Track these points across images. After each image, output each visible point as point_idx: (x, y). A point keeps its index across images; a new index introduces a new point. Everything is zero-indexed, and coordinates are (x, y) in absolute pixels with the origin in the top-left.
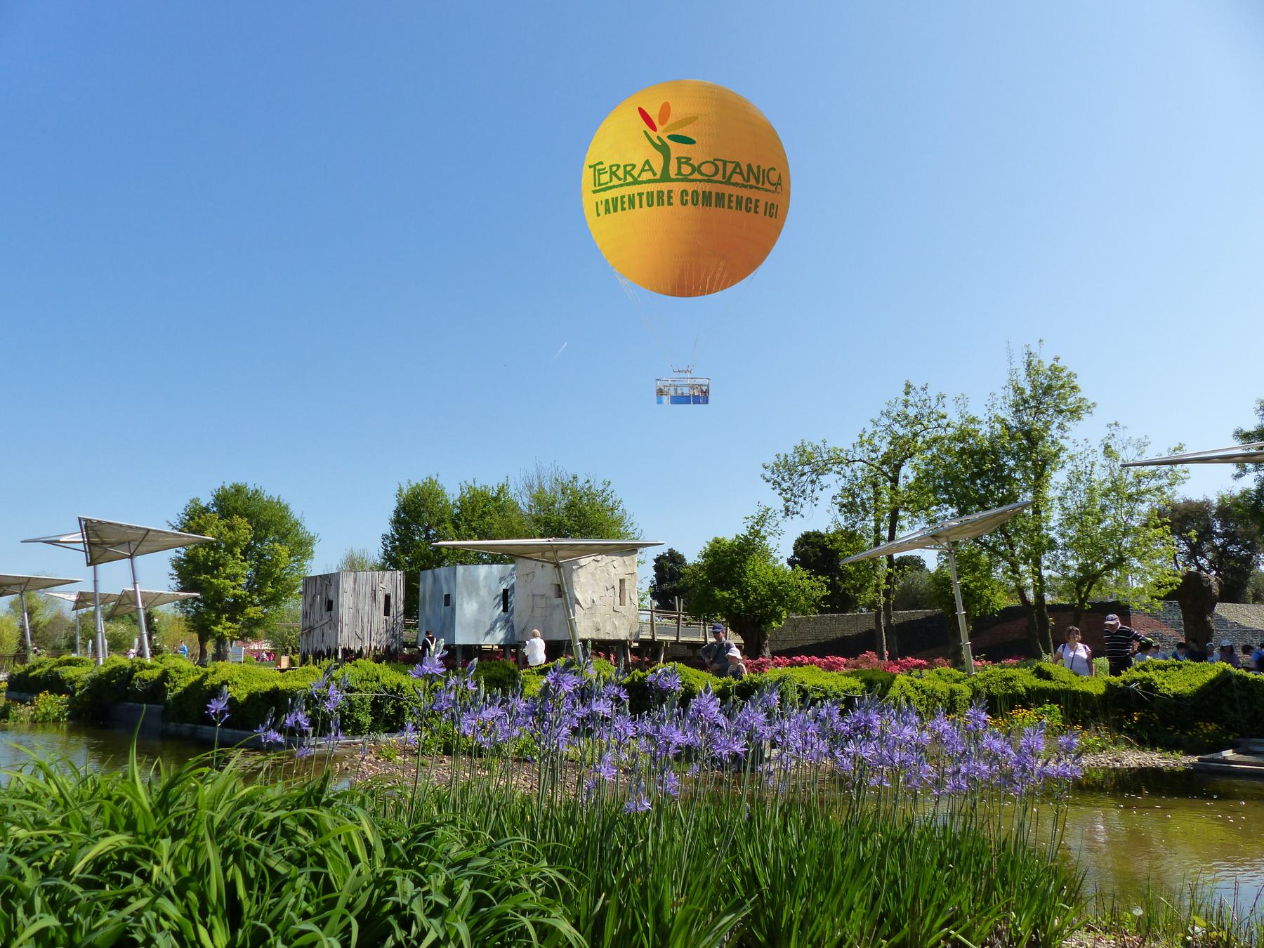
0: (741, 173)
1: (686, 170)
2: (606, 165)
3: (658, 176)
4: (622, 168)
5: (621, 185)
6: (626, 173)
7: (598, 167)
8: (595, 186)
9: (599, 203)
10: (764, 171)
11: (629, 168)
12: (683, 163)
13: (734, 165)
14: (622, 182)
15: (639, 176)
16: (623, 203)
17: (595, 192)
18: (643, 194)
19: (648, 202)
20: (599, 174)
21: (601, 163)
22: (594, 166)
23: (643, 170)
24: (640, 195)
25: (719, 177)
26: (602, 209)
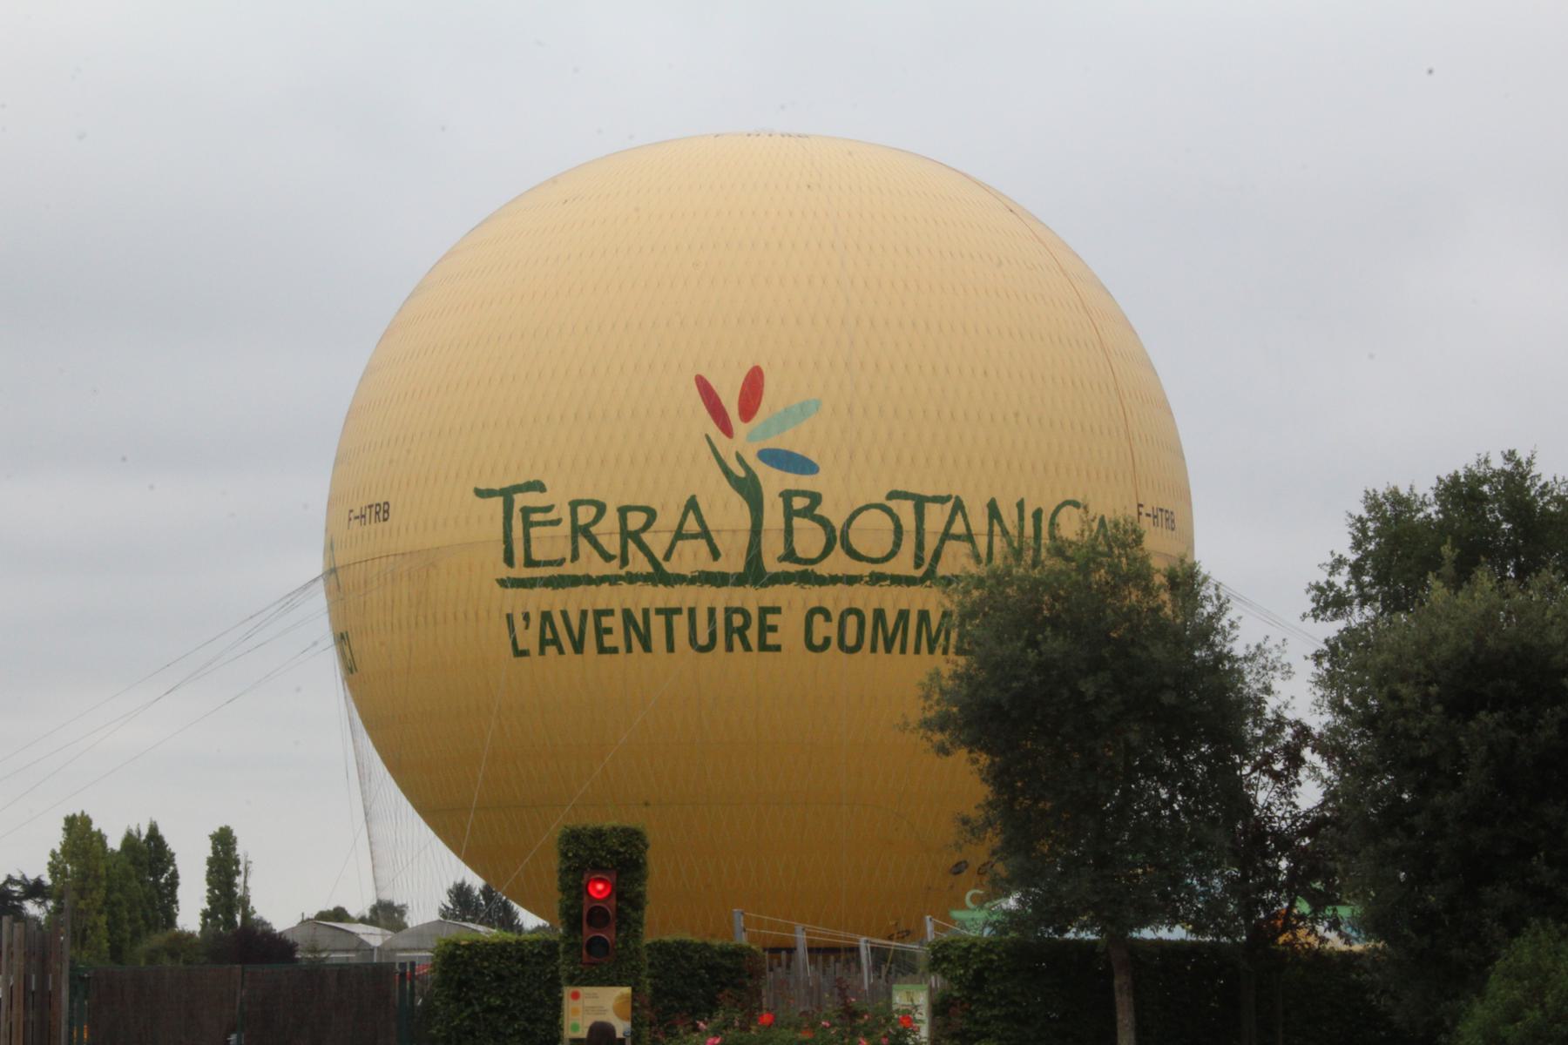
0: (969, 537)
1: (809, 539)
2: (558, 496)
3: (734, 563)
4: (610, 521)
5: (612, 580)
6: (626, 535)
7: (520, 500)
8: (509, 559)
9: (519, 623)
10: (1037, 515)
11: (636, 521)
12: (800, 513)
13: (950, 505)
14: (613, 568)
15: (667, 557)
16: (601, 632)
17: (503, 583)
18: (678, 611)
19: (693, 639)
20: (528, 525)
21: (538, 486)
22: (507, 494)
23: (680, 535)
24: (669, 613)
25: (903, 564)
26: (529, 638)
